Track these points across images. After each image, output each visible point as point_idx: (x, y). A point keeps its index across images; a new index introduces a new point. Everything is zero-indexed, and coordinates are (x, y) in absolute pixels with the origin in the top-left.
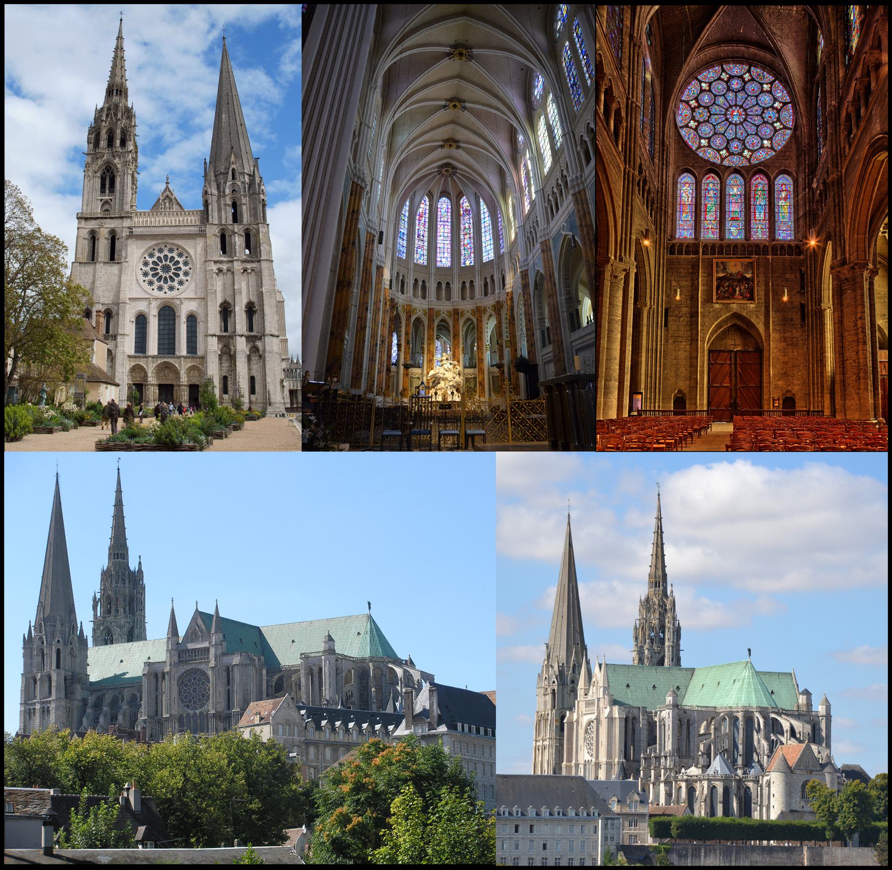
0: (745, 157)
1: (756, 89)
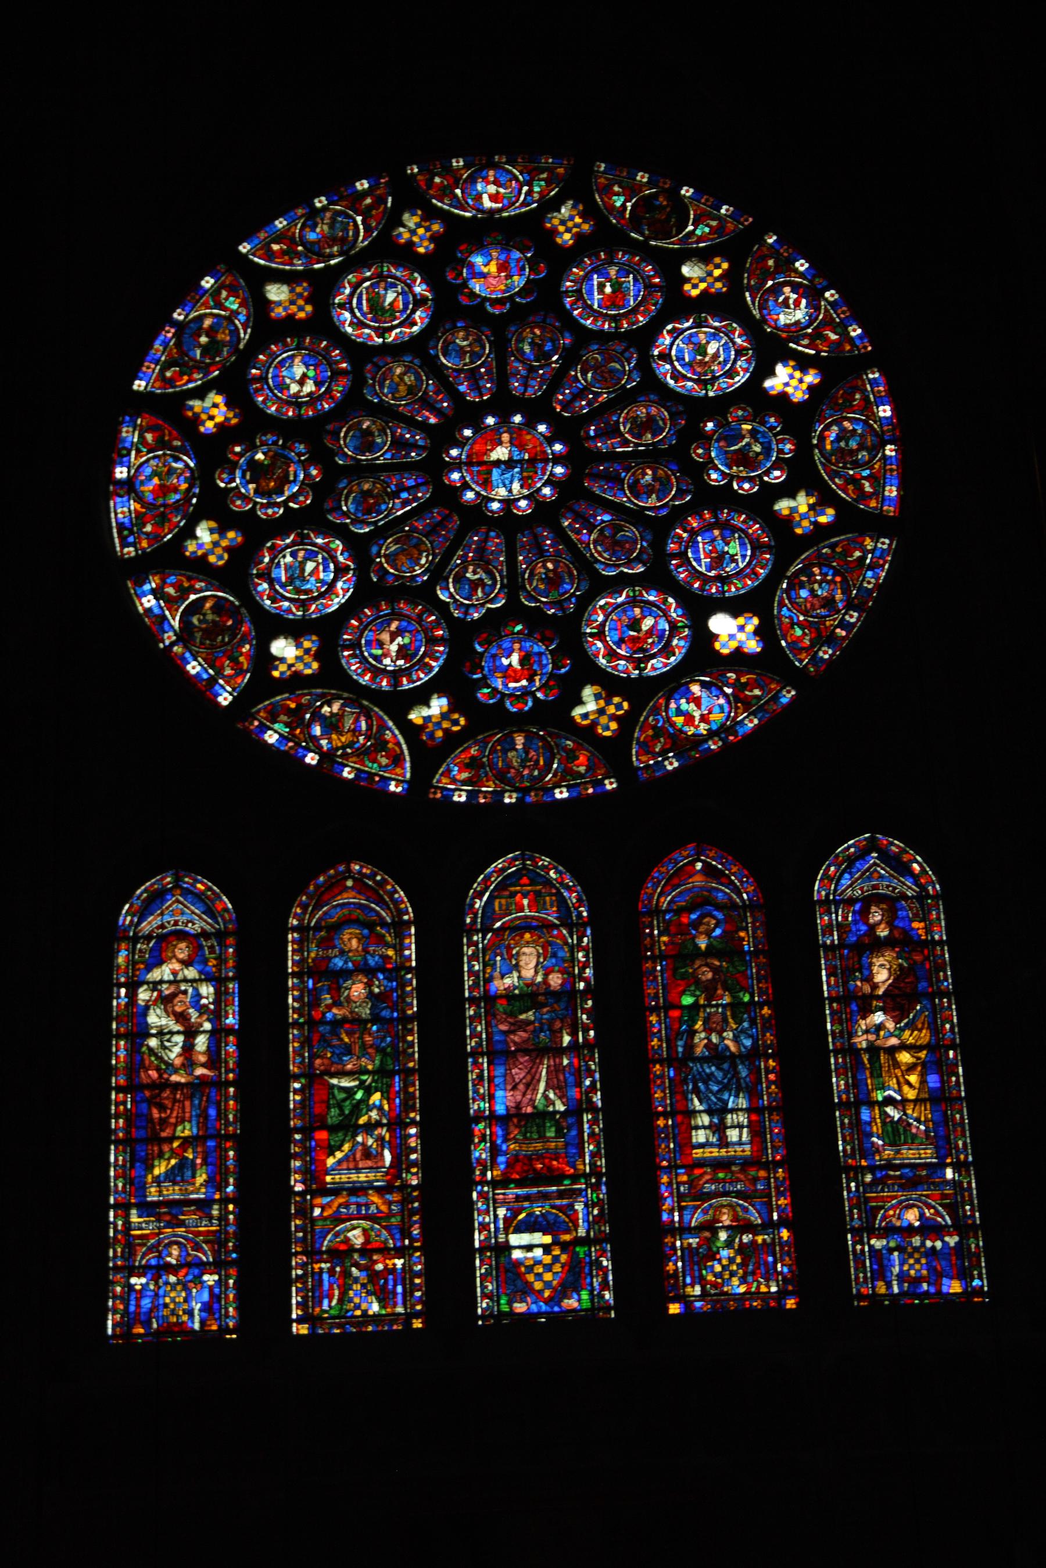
0: (587, 734)
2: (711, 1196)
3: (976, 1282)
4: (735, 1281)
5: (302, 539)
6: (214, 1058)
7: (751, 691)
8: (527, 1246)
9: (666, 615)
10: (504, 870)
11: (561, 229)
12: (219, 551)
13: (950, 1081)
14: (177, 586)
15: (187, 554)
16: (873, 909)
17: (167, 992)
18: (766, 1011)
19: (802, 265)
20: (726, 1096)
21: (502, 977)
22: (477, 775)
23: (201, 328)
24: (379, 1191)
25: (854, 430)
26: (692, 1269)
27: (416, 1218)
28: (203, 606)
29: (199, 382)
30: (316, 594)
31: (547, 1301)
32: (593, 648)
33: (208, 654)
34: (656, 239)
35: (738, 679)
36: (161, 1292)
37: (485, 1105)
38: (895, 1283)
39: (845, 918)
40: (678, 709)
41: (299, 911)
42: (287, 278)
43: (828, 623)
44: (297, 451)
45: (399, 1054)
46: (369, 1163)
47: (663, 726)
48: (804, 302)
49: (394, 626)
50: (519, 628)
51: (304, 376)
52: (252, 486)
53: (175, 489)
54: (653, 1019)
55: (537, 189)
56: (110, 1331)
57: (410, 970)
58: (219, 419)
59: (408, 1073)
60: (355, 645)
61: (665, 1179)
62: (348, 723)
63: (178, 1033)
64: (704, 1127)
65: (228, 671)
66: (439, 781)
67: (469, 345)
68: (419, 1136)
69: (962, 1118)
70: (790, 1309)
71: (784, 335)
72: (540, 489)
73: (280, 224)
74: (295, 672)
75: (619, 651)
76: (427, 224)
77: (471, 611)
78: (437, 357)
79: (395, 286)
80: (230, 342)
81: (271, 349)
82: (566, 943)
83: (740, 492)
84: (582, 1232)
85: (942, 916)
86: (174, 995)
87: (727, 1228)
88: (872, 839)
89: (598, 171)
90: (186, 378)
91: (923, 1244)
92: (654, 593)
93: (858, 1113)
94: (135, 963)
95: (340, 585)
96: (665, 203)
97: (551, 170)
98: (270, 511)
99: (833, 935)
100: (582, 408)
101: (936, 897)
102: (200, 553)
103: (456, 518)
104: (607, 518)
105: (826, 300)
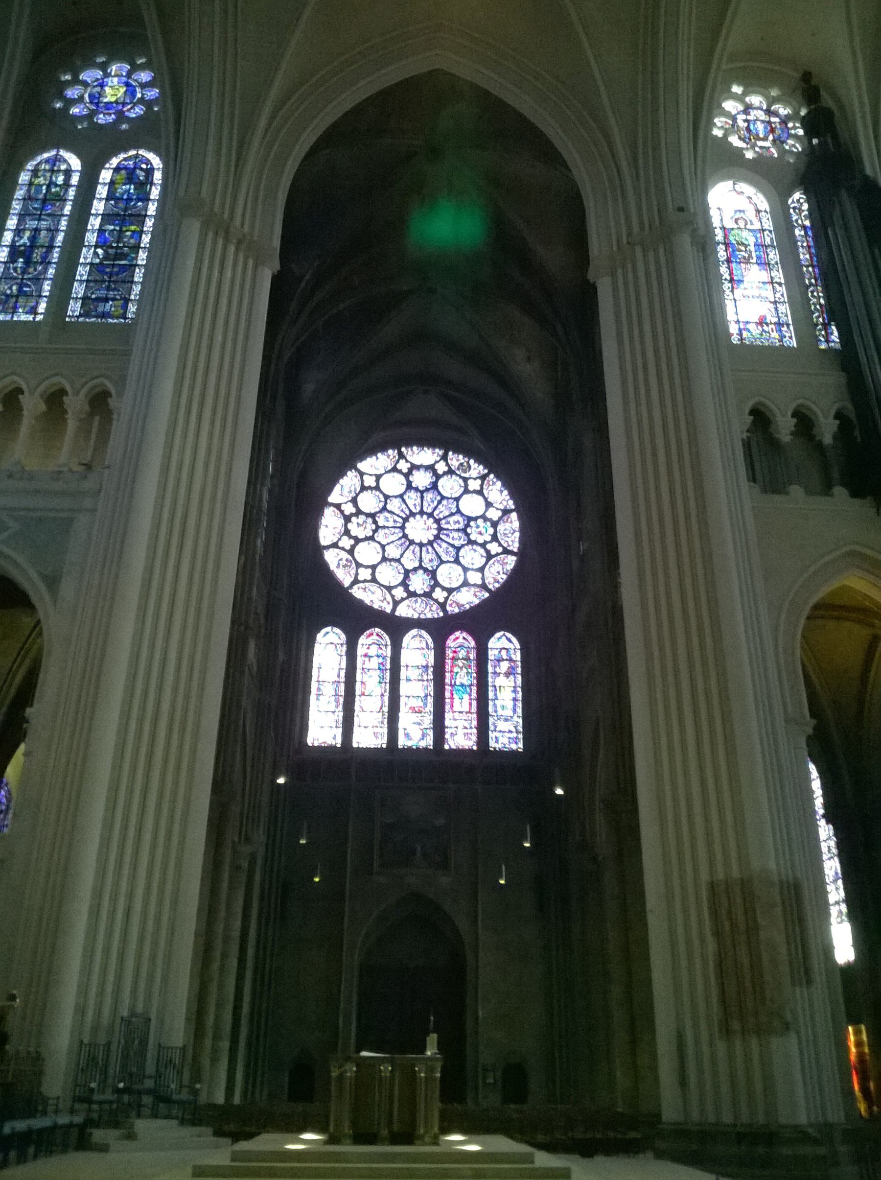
0: (436, 601)
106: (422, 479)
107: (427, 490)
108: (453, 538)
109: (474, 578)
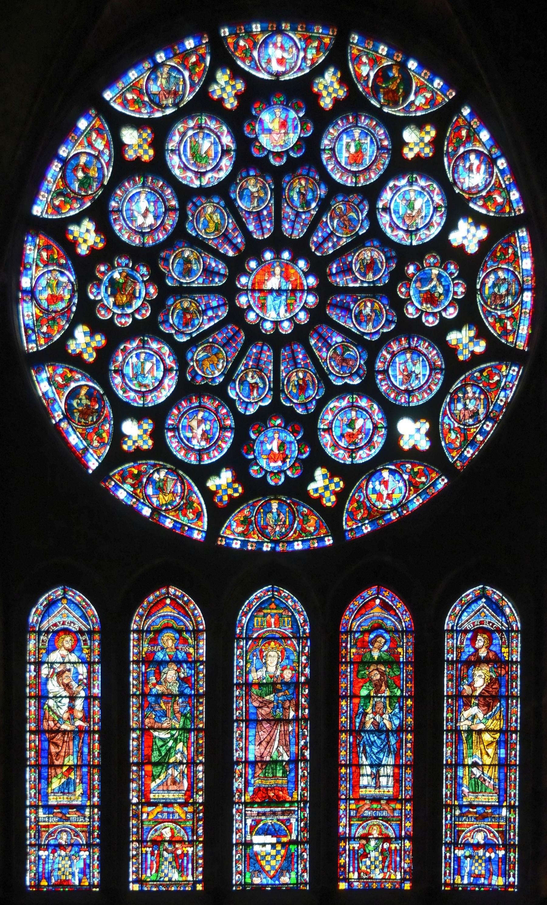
0: (316, 503)
1: (370, 151)
2: (367, 818)
3: (511, 879)
4: (377, 871)
5: (143, 345)
6: (86, 718)
7: (420, 478)
8: (262, 844)
9: (371, 418)
10: (260, 598)
11: (324, 93)
12: (90, 350)
13: (511, 754)
14: (63, 376)
15: (70, 351)
16: (479, 637)
17: (59, 670)
18: (409, 702)
19: (485, 135)
20: (381, 756)
21: (257, 671)
22: (247, 529)
23: (78, 165)
24: (181, 805)
25: (505, 279)
26: (354, 863)
27: (201, 823)
28: (79, 393)
29: (77, 211)
30: (151, 388)
31: (271, 878)
32: (325, 440)
33: (83, 430)
34: (388, 106)
35: (412, 469)
36: (57, 861)
37: (242, 754)
38: (466, 877)
39: (462, 643)
40: (374, 489)
41: (138, 619)
42: (138, 124)
43: (472, 430)
44: (141, 273)
45: (193, 719)
46: (175, 787)
47: (363, 501)
48: (483, 167)
49: (201, 414)
50: (279, 421)
51: (147, 210)
52: (112, 300)
53: (62, 299)
54: (343, 703)
55: (309, 56)
56: (28, 883)
57: (202, 663)
58: (91, 243)
59: (199, 730)
60: (175, 429)
61: (343, 807)
62: (170, 486)
63: (66, 697)
64: (368, 775)
65: (96, 443)
66: (224, 533)
67: (258, 191)
68: (205, 772)
69: (515, 778)
70: (407, 890)
71: (466, 196)
72: (297, 314)
73: (133, 75)
74: (138, 447)
75: (340, 443)
76: (234, 83)
77: (249, 407)
78: (235, 199)
79: (208, 135)
80: (97, 178)
81: (125, 186)
82: (295, 650)
83: (427, 324)
84: (294, 837)
85: (519, 645)
86: (63, 672)
87: (376, 839)
88: (484, 589)
89: (353, 43)
90: (68, 207)
91: (484, 855)
92: (365, 400)
93: (456, 772)
94: (39, 649)
95: (166, 381)
96: (396, 75)
97: (320, 39)
98: (123, 321)
99: (453, 653)
100: (328, 248)
101: (517, 631)
102: (78, 351)
103: (243, 334)
104: (339, 339)
105: (498, 167)
106: (277, 131)
107: (292, 167)
108: (360, 318)
109: (413, 433)
